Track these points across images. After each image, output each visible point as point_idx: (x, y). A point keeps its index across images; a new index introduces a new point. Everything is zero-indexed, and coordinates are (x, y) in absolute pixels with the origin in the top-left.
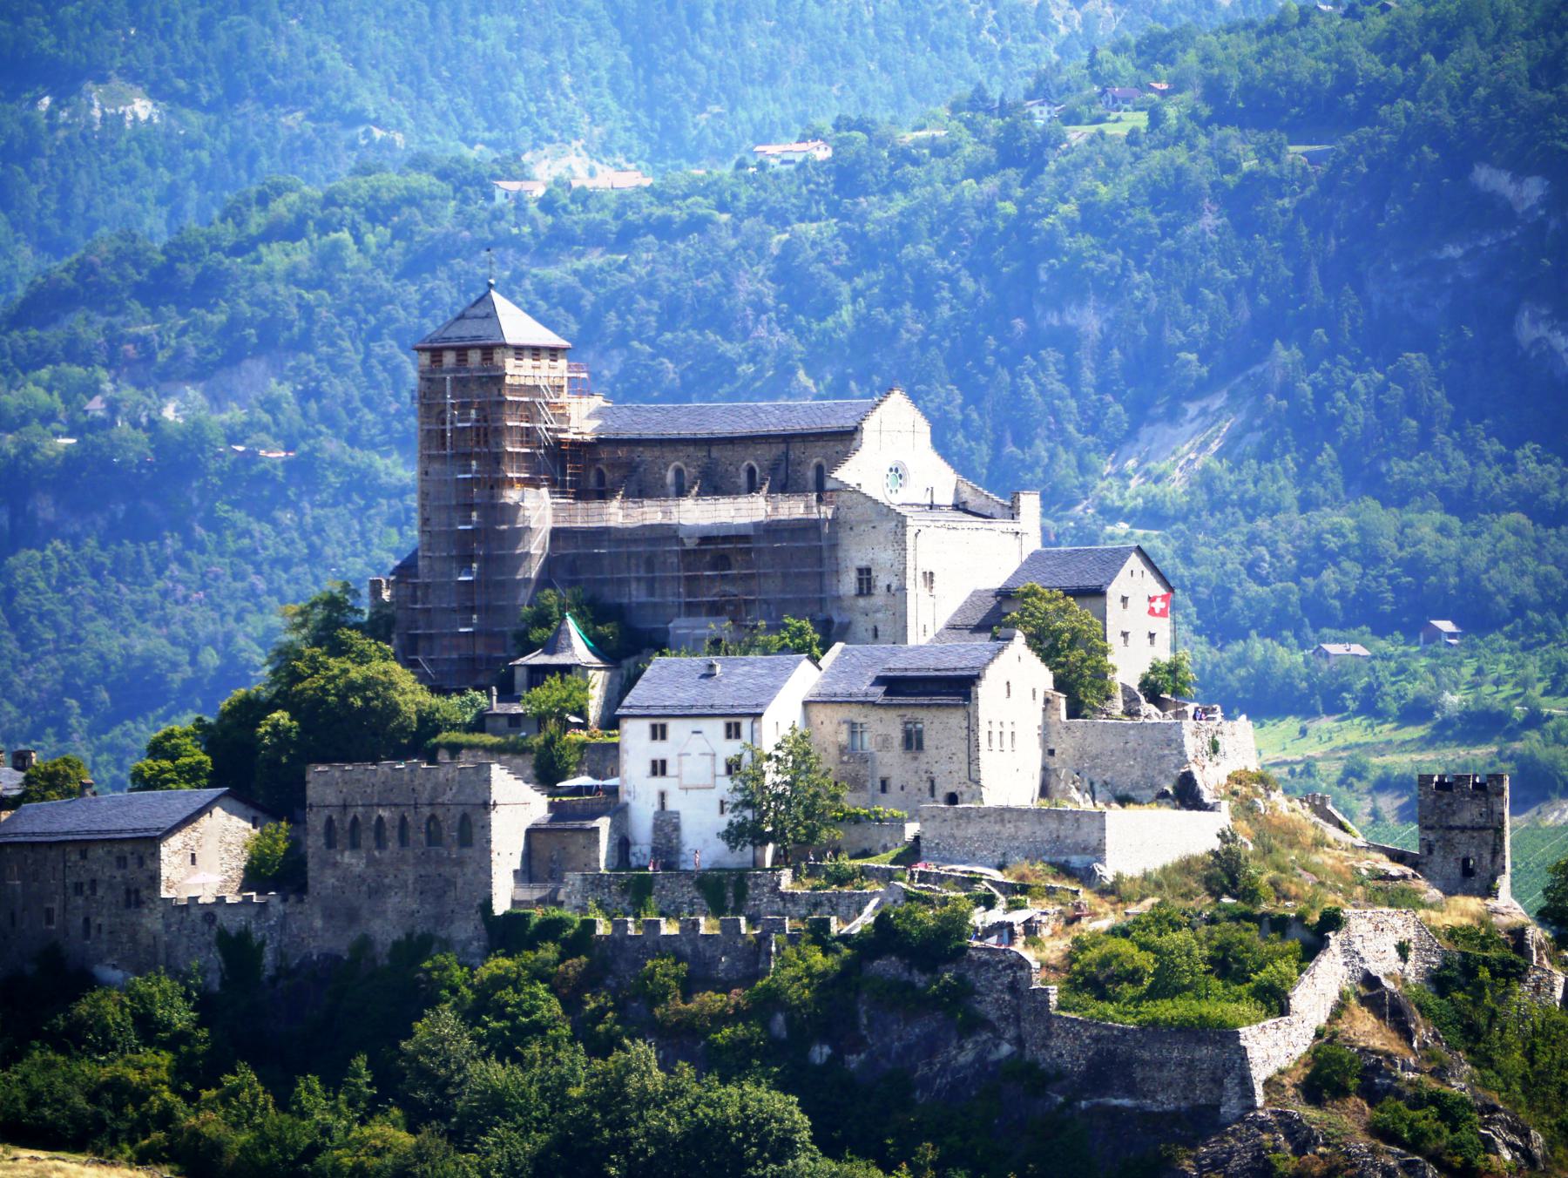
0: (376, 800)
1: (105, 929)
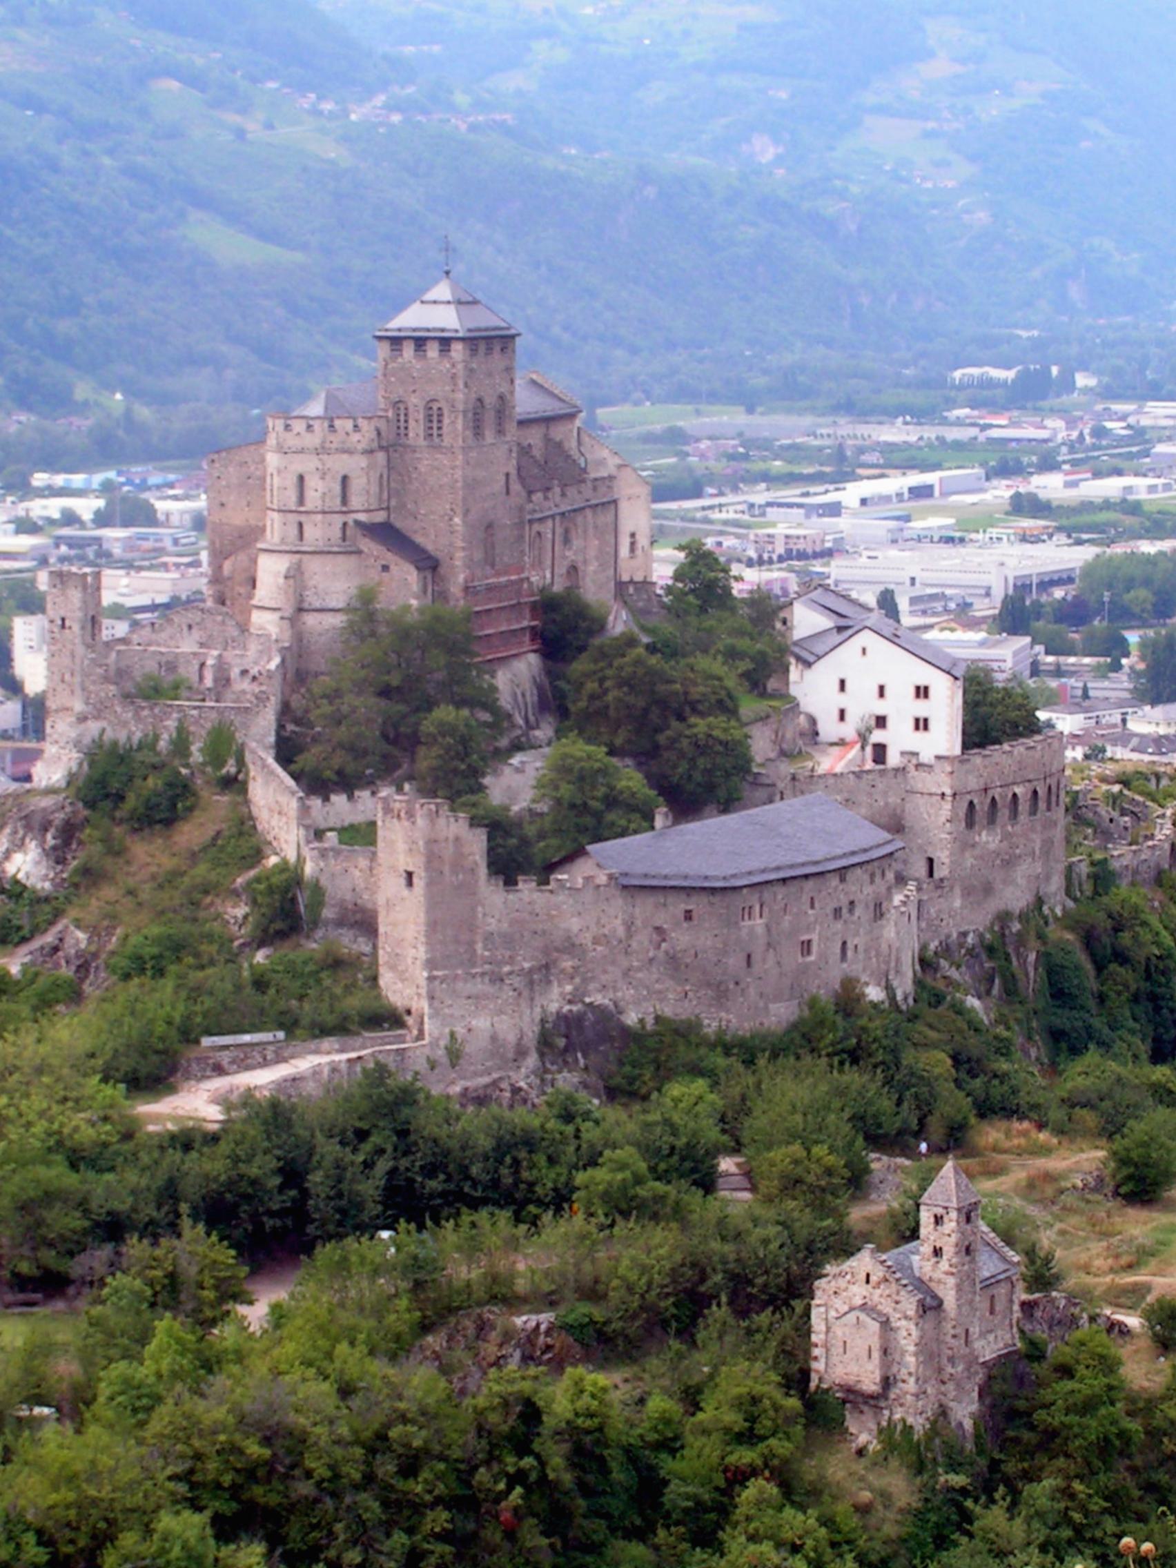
0: (1010, 780)
1: (861, 949)
